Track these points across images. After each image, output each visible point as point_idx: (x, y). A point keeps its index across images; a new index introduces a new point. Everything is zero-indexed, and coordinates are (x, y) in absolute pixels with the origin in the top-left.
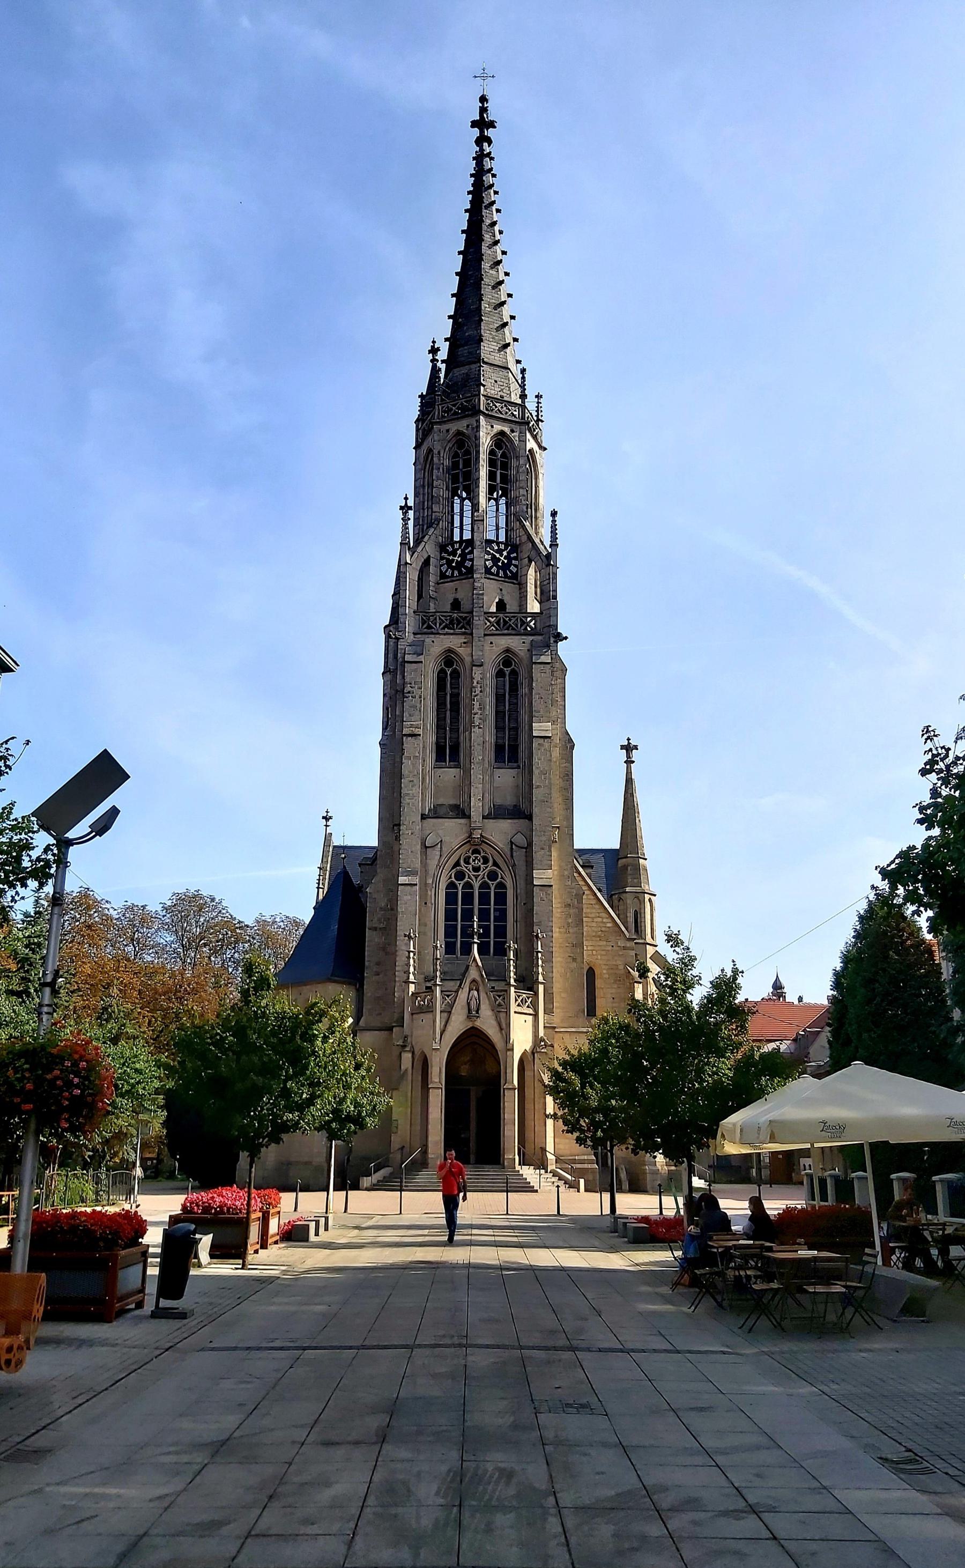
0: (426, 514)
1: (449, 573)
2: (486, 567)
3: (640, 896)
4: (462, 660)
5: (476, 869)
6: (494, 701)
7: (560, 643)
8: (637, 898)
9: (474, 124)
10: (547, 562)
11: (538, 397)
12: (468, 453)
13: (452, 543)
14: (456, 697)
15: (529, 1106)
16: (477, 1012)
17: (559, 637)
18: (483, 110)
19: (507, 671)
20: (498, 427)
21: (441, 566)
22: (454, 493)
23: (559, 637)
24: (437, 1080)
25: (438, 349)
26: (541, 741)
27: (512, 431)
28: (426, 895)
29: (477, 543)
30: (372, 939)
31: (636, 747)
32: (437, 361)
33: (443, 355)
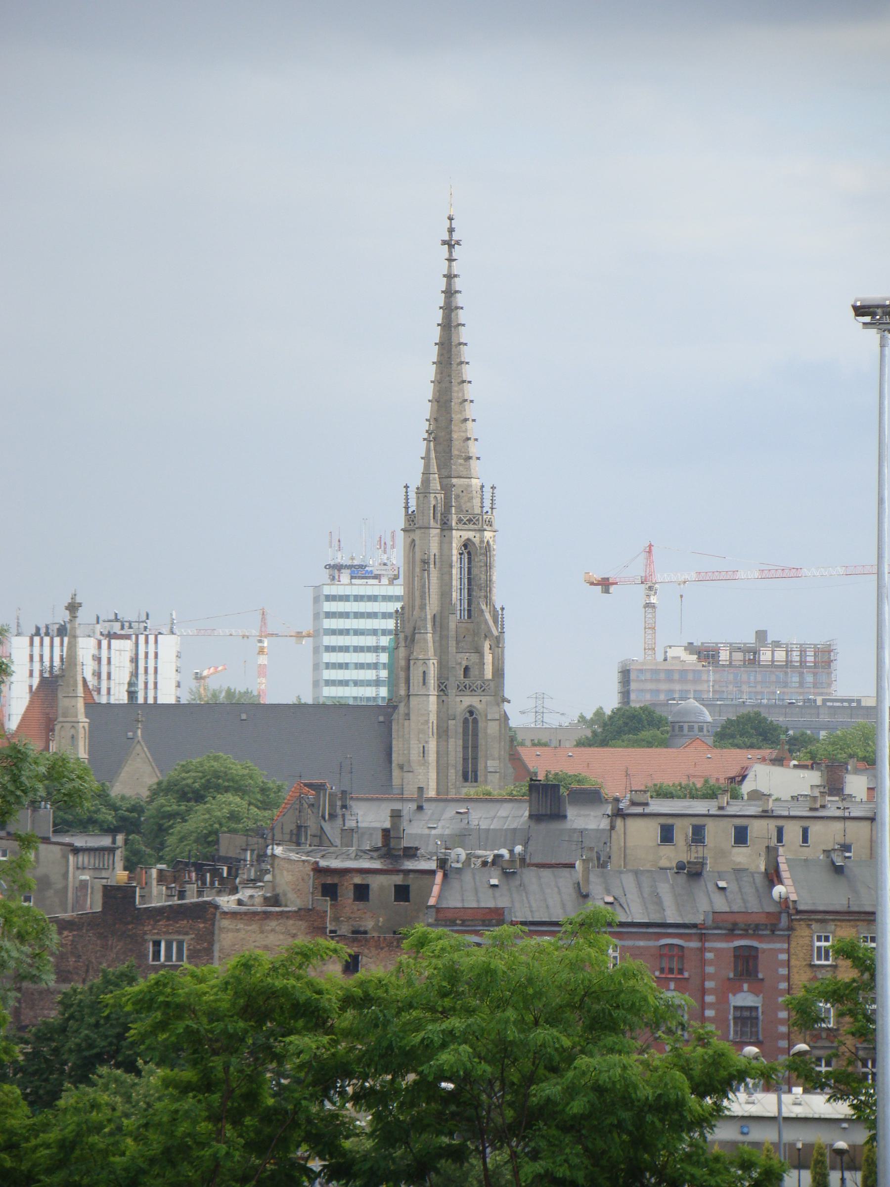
9: (444, 243)
10: (498, 642)
11: (493, 488)
17: (505, 700)
18: (451, 230)
19: (470, 719)
23: (505, 700)
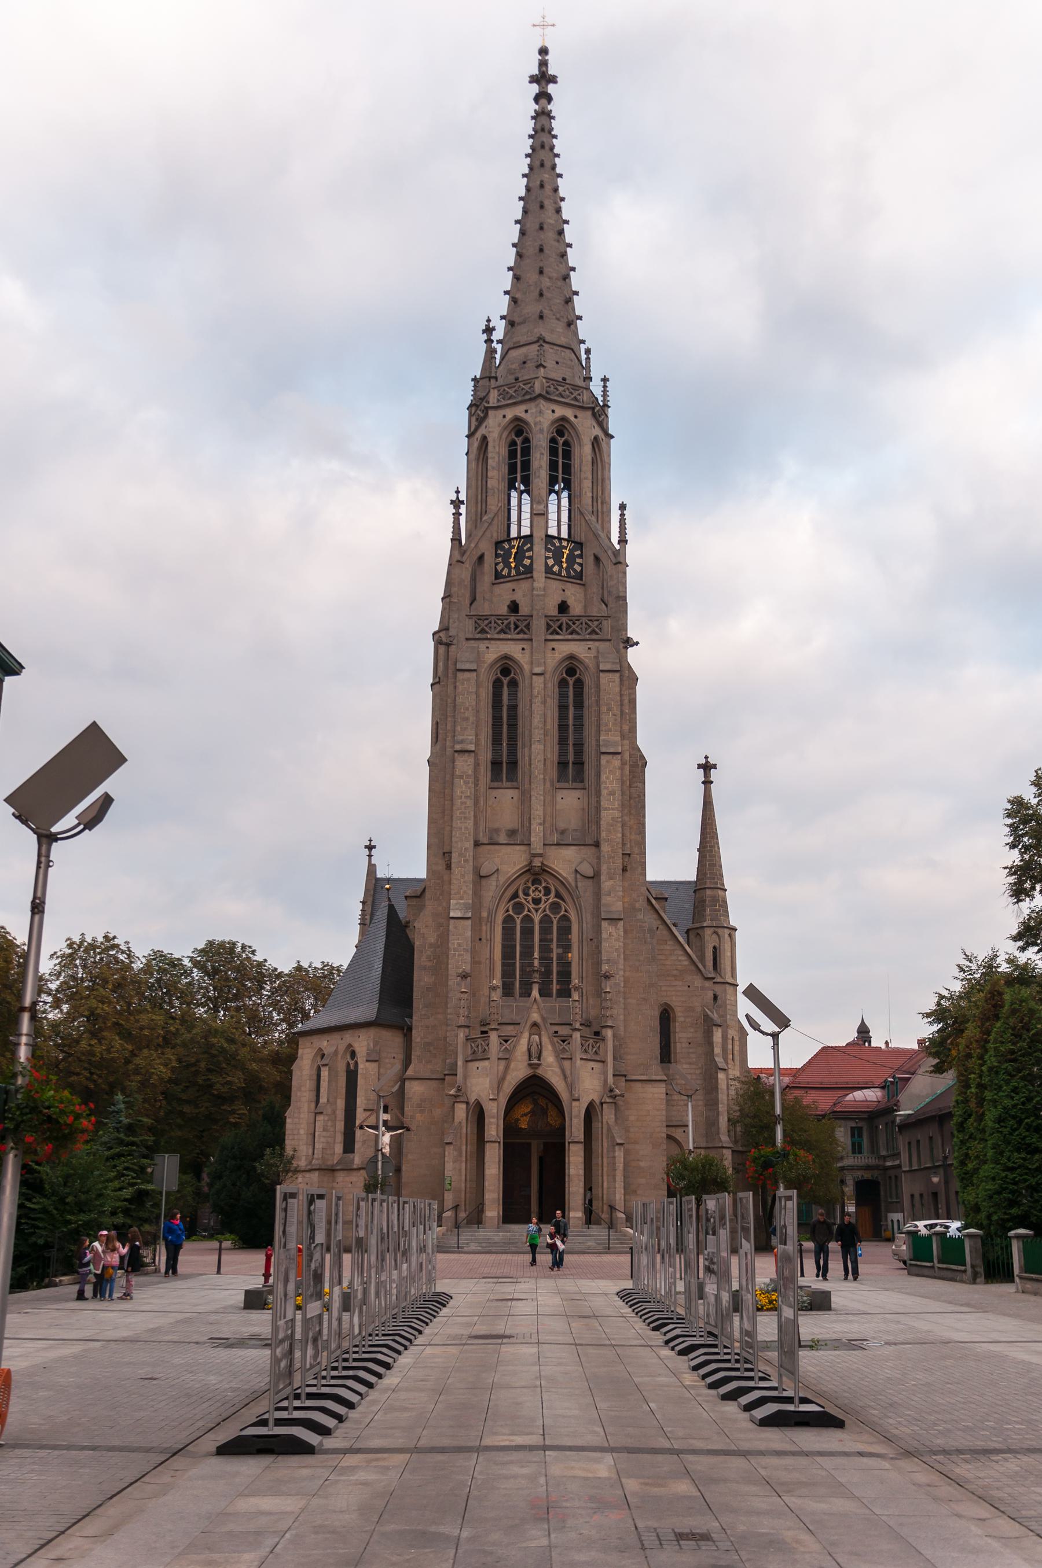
0: (479, 506)
1: (505, 572)
2: (546, 563)
3: (720, 931)
4: (521, 668)
5: (537, 901)
6: (556, 714)
7: (630, 650)
8: (715, 932)
9: (533, 79)
11: (605, 380)
12: (527, 440)
13: (509, 540)
14: (513, 709)
15: (596, 1160)
16: (539, 1060)
17: (629, 643)
18: (543, 64)
19: (571, 681)
20: (561, 411)
21: (497, 564)
22: (511, 486)
23: (629, 643)
24: (494, 1133)
25: (494, 329)
26: (610, 757)
27: (576, 417)
28: (481, 930)
29: (536, 540)
30: (422, 979)
31: (714, 766)
32: (492, 341)
33: (498, 334)
